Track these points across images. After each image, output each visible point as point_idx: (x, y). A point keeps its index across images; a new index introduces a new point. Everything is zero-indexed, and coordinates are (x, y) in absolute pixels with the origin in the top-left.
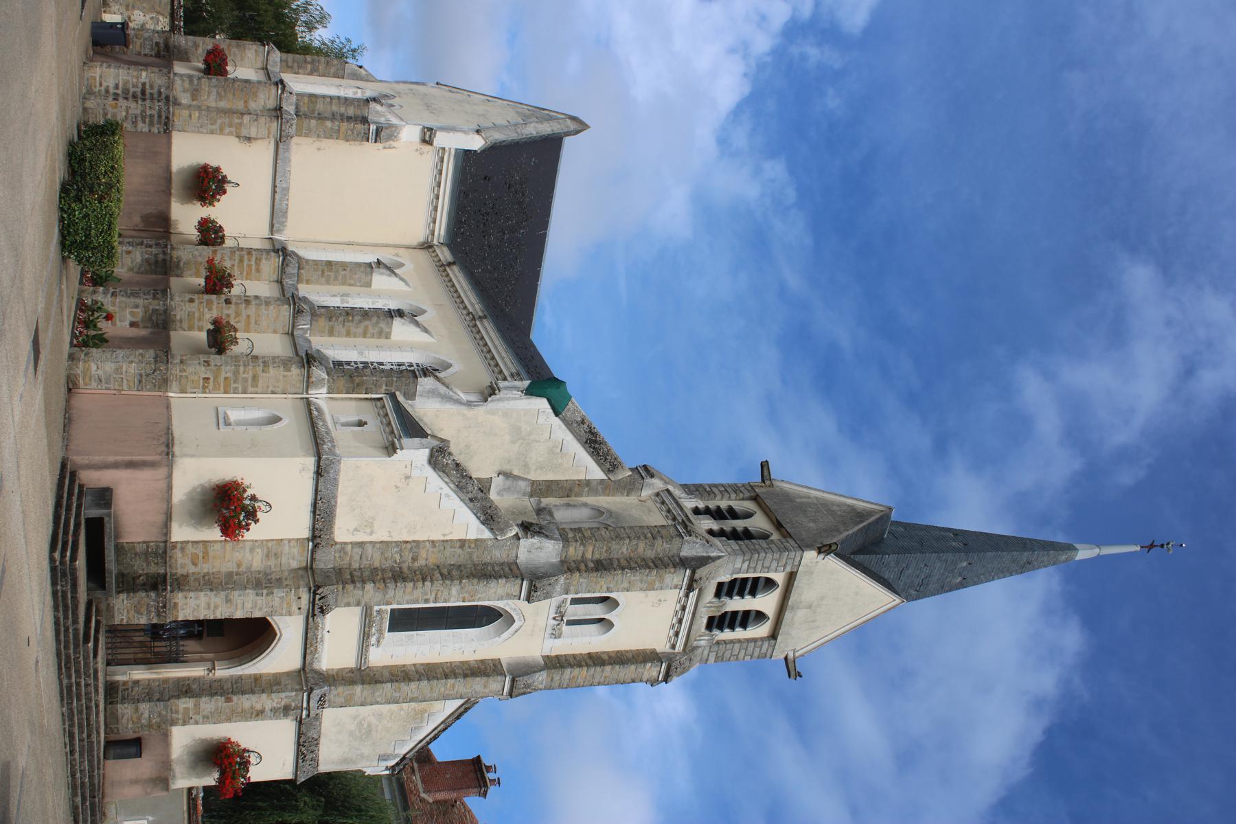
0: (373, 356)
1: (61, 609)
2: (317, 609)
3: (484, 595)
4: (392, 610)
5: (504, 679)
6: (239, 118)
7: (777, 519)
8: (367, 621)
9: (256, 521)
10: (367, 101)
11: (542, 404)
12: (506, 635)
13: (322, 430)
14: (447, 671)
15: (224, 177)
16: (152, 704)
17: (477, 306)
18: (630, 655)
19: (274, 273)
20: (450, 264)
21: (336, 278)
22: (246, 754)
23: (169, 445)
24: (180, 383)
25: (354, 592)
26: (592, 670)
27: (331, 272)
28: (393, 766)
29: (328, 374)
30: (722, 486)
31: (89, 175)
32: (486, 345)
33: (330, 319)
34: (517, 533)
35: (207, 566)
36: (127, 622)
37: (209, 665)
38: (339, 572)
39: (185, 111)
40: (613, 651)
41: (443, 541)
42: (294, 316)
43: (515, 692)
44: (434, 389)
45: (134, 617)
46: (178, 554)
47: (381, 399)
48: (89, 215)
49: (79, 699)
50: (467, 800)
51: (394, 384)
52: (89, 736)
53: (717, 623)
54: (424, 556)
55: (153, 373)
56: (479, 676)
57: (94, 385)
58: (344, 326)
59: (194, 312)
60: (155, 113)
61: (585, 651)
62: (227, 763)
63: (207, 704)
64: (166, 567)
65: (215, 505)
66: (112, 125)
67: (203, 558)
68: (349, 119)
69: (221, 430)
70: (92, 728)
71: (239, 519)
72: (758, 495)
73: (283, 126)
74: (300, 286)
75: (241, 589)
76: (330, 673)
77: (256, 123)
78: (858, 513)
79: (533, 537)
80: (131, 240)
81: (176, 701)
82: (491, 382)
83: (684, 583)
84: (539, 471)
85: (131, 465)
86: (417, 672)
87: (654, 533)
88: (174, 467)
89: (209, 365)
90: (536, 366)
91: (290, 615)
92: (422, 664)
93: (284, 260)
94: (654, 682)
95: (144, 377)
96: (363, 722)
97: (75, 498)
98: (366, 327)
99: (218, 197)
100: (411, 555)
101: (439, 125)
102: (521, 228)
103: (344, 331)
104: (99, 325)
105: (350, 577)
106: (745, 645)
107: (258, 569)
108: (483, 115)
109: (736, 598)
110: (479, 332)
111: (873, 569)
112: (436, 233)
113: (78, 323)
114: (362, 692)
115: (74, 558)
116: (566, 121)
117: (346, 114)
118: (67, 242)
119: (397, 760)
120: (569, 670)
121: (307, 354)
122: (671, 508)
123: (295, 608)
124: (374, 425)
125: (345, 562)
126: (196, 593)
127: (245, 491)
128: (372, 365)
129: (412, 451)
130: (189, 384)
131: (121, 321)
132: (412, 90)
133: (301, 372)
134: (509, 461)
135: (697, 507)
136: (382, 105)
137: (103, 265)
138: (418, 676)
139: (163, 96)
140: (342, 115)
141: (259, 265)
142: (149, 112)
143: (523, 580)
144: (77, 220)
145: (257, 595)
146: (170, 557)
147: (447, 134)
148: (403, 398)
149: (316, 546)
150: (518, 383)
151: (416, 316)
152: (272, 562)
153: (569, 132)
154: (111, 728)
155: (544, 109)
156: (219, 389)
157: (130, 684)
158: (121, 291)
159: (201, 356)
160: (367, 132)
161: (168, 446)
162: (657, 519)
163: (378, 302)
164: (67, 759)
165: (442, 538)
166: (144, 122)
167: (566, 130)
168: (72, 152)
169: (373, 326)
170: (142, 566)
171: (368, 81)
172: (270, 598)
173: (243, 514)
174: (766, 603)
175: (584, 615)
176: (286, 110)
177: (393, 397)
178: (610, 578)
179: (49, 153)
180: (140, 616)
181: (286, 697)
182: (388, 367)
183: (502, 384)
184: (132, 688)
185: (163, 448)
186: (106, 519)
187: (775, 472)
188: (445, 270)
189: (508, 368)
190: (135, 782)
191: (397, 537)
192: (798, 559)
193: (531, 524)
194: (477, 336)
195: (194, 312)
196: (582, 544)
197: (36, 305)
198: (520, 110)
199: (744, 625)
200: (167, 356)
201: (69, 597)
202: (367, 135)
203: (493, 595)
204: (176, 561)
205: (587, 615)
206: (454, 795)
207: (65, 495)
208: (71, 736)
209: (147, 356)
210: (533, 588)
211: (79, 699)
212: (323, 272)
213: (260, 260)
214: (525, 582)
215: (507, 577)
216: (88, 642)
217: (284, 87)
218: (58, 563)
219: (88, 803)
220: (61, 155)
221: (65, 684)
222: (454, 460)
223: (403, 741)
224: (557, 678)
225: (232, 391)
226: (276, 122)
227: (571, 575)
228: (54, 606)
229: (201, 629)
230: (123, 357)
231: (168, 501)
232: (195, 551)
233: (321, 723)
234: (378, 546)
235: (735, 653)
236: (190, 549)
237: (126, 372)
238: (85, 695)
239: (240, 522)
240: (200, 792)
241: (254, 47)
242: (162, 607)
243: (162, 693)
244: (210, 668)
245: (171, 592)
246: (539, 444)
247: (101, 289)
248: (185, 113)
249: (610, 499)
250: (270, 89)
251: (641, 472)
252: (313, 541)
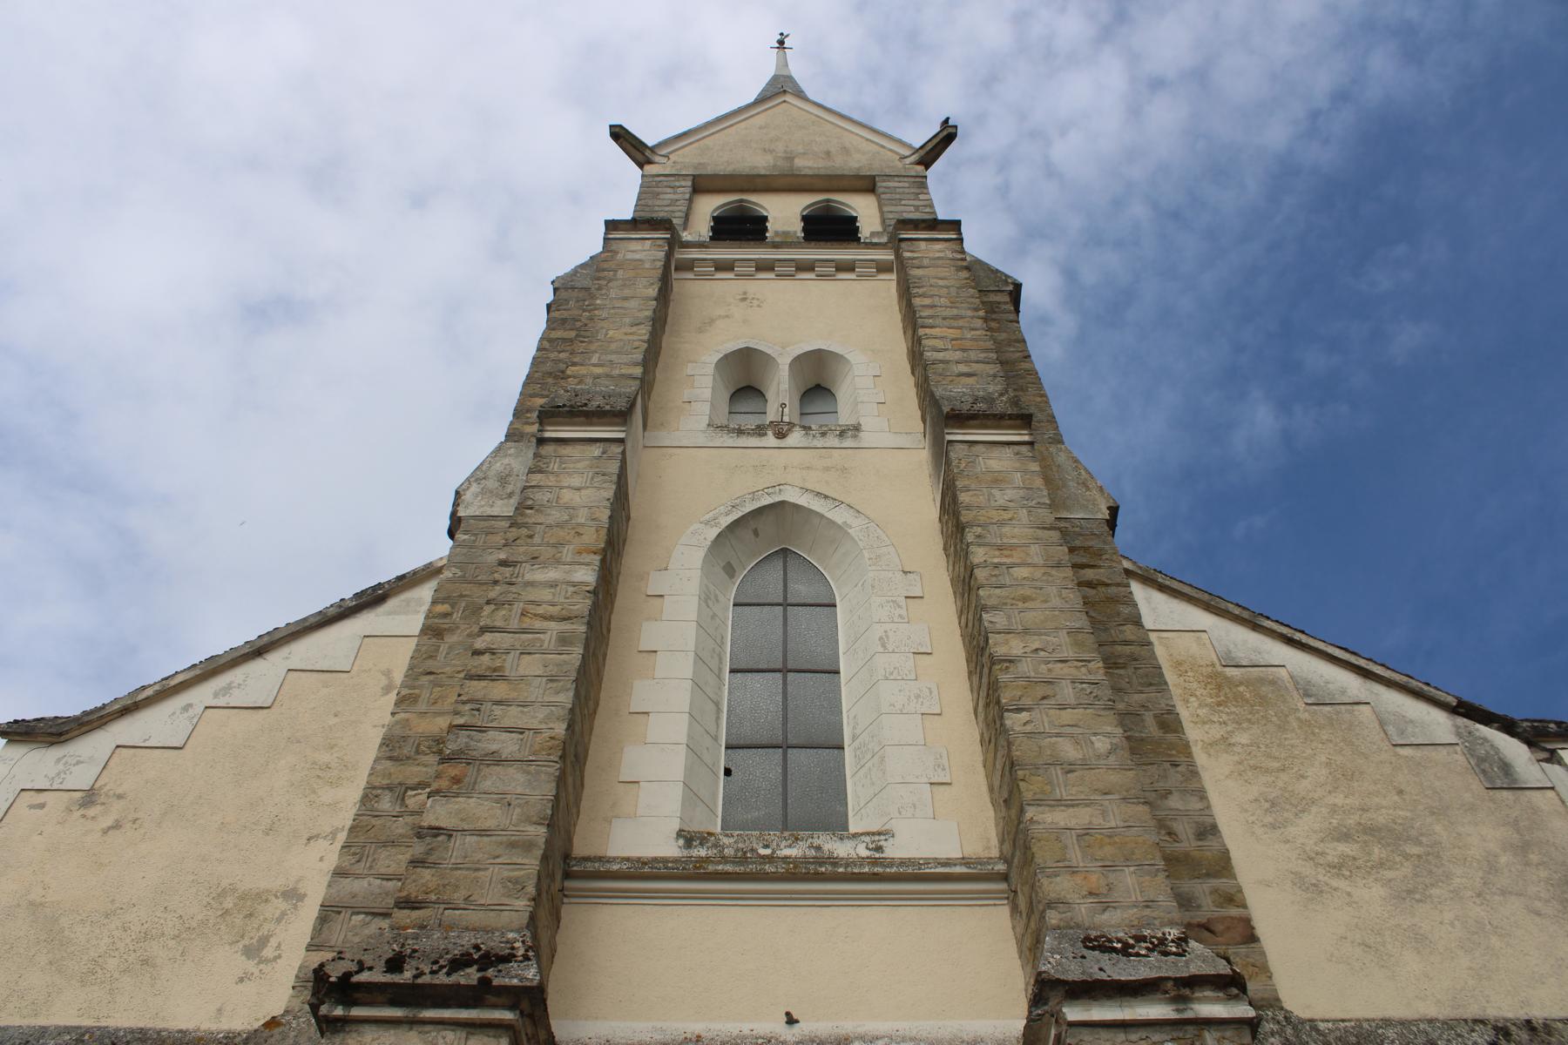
8: (729, 868)
12: (838, 516)
28: (1530, 744)
96: (1332, 858)
223: (1382, 724)
233: (1387, 1022)
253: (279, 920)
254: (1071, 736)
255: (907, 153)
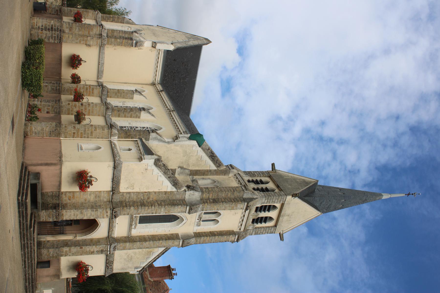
0: (134, 124)
1: (21, 217)
2: (114, 216)
3: (173, 211)
4: (140, 216)
5: (180, 241)
6: (86, 38)
7: (277, 184)
8: (131, 220)
9: (92, 185)
10: (132, 32)
11: (195, 143)
13: (116, 152)
14: (159, 238)
15: (81, 59)
16: (54, 249)
17: (171, 107)
18: (225, 232)
19: (98, 94)
20: (161, 91)
21: (121, 96)
22: (87, 266)
23: (61, 157)
24: (65, 134)
25: (127, 210)
26: (211, 238)
27: (119, 94)
28: (140, 271)
29: (118, 132)
30: (258, 172)
31: (32, 59)
32: (174, 121)
33: (119, 111)
34: (185, 189)
35: (74, 200)
36: (45, 220)
37: (75, 235)
38: (121, 202)
39: (66, 35)
40: (219, 231)
41: (159, 192)
42: (106, 110)
43: (184, 245)
44: (156, 137)
45: (48, 218)
46: (64, 196)
47: (137, 141)
48: (32, 74)
49: (28, 249)
50: (165, 280)
51: (142, 135)
52: (31, 261)
53: (256, 221)
54: (152, 197)
55: (55, 131)
56: (171, 240)
57: (34, 135)
58: (123, 114)
59: (70, 108)
60: (56, 36)
61: (209, 231)
62: (80, 270)
63: (74, 249)
64: (59, 201)
65: (77, 179)
66: (40, 40)
67: (73, 197)
68: (126, 38)
69: (79, 152)
70: (32, 258)
71: (86, 184)
72: (270, 175)
73: (102, 41)
74: (108, 99)
75: (86, 209)
76: (118, 238)
77: (92, 40)
78: (306, 182)
79: (191, 191)
80: (47, 81)
81: (63, 248)
82: (176, 135)
83: (245, 207)
84: (193, 167)
85: (47, 164)
86: (149, 238)
87: (234, 189)
88: (62, 165)
89: (75, 128)
90: (192, 128)
91: (104, 218)
92: (151, 235)
93: (102, 89)
94: (233, 242)
95: (52, 132)
97: (26, 177)
98: (132, 114)
99: (79, 66)
100: (147, 197)
101: (158, 41)
102: (187, 78)
103: (123, 115)
104: (36, 113)
105: (125, 205)
106: (265, 229)
107: (92, 202)
108: (174, 37)
109: (263, 212)
110: (172, 116)
111: (311, 202)
112: (157, 80)
113: (28, 112)
114: (129, 245)
115: (26, 199)
116: (203, 40)
117: (125, 37)
118: (24, 84)
119: (141, 269)
120: (203, 238)
121: (110, 124)
122: (240, 180)
123: (105, 216)
124: (134, 150)
125: (123, 199)
126: (70, 210)
127: (88, 174)
128: (134, 128)
129: (148, 160)
130: (68, 135)
131: (43, 111)
132: (148, 28)
133: (108, 131)
134: (182, 163)
135: (249, 180)
136: (138, 34)
137: (37, 92)
138: (149, 240)
139: (59, 29)
140: (123, 37)
141: (93, 91)
142: (54, 35)
143: (187, 206)
144: (28, 76)
145: (92, 211)
146: (61, 197)
147: (161, 44)
148: (145, 140)
149: (113, 194)
150: (186, 135)
151: (149, 110)
152: (97, 199)
153: (204, 44)
154: (39, 258)
155: (195, 36)
156: (79, 137)
157: (46, 242)
158: (43, 100)
159: (72, 125)
160: (132, 43)
161: (60, 158)
162: (235, 184)
163: (136, 105)
164: (23, 270)
165: (158, 191)
166: (52, 39)
167: (203, 43)
168: (26, 50)
169: (134, 114)
170: (51, 200)
171: (132, 24)
172: (96, 212)
173: (87, 182)
174: (273, 214)
175: (208, 218)
176: (103, 35)
177: (141, 140)
178: (218, 205)
179: (18, 52)
180: (50, 218)
181: (102, 247)
182: (139, 129)
183: (180, 135)
184: (47, 243)
185: (59, 158)
186: (38, 184)
187: (277, 168)
188: (160, 93)
189: (182, 130)
190: (47, 276)
191: (142, 191)
192: (285, 199)
193: (190, 186)
194: (171, 118)
195: (70, 108)
196: (208, 193)
197: (13, 108)
198: (187, 36)
199: (265, 222)
200: (60, 125)
201: (24, 213)
202: (132, 45)
203: (176, 211)
204: (63, 199)
205: (209, 218)
206: (161, 279)
207: (23, 176)
208: (25, 261)
209: (53, 124)
210: (191, 209)
211: (28, 249)
212: (116, 93)
213: (94, 89)
214: (188, 207)
215: (181, 205)
216: (31, 228)
217: (103, 27)
218: (20, 201)
219: (31, 285)
220: (22, 52)
221: (22, 243)
222: (163, 163)
223: (143, 262)
224: (198, 240)
225: (83, 138)
226: (100, 40)
227: (204, 204)
228: (19, 216)
229: (71, 222)
230: (44, 125)
231: (60, 177)
232: (70, 195)
233: (114, 256)
234: (135, 193)
235: (262, 231)
236: (68, 194)
237: (45, 130)
238: (30, 247)
239: (86, 185)
240: (71, 279)
241: (92, 12)
242: (58, 215)
243: (57, 245)
244: (75, 236)
245: (61, 210)
246: (193, 157)
247: (36, 99)
248: (67, 36)
249: (218, 176)
250: (98, 28)
251: (229, 167)
252: (112, 191)
253: (131, 189)
254: (136, 246)
255: (284, 232)
